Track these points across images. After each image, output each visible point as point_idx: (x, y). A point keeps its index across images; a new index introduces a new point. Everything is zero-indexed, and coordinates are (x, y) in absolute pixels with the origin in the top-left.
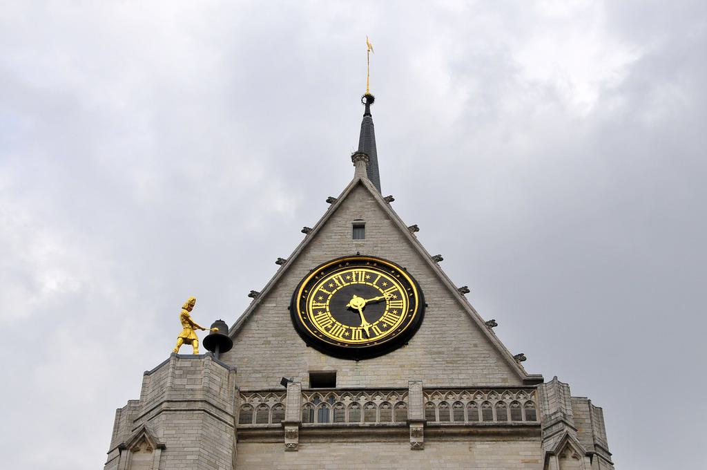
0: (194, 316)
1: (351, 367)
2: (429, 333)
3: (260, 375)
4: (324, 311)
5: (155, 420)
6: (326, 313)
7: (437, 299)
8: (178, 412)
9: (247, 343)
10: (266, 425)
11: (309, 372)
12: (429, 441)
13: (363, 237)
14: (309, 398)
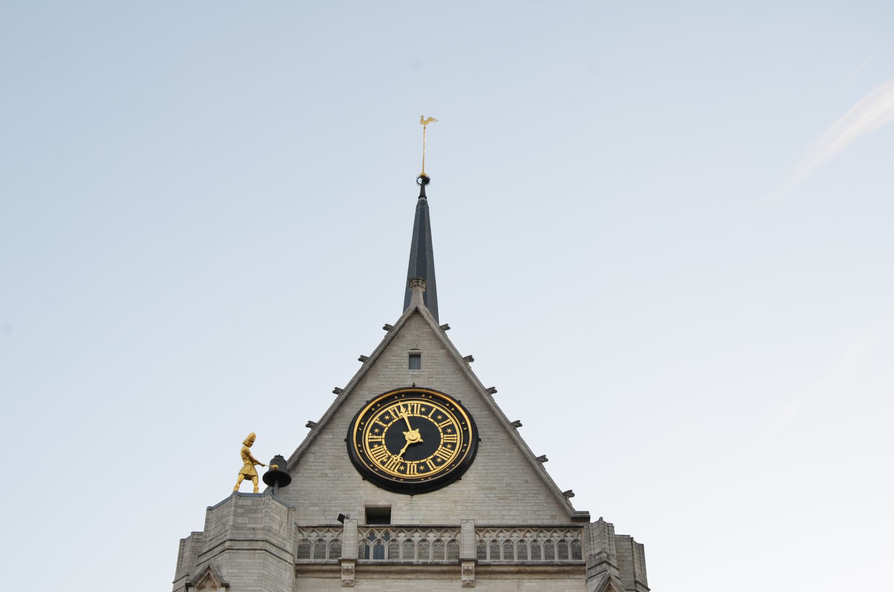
0: (254, 451)
1: (406, 502)
2: (483, 468)
3: (317, 509)
4: (380, 444)
5: (219, 558)
6: (381, 447)
7: (490, 433)
8: (240, 551)
9: (305, 475)
10: (323, 561)
11: (365, 505)
12: (480, 578)
13: (419, 368)
14: (365, 534)
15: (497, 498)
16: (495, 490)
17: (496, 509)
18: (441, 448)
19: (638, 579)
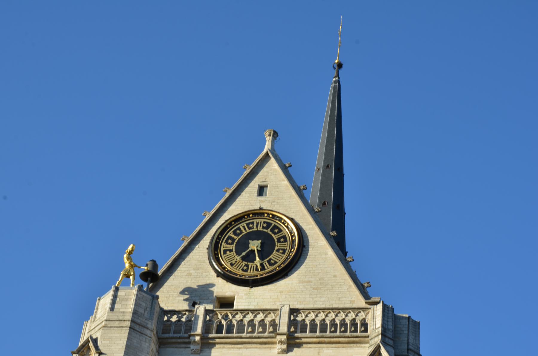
4: (231, 251)
6: (232, 253)
8: (112, 328)
10: (179, 335)
15: (312, 289)
16: (312, 282)
17: (311, 296)
19: (410, 347)
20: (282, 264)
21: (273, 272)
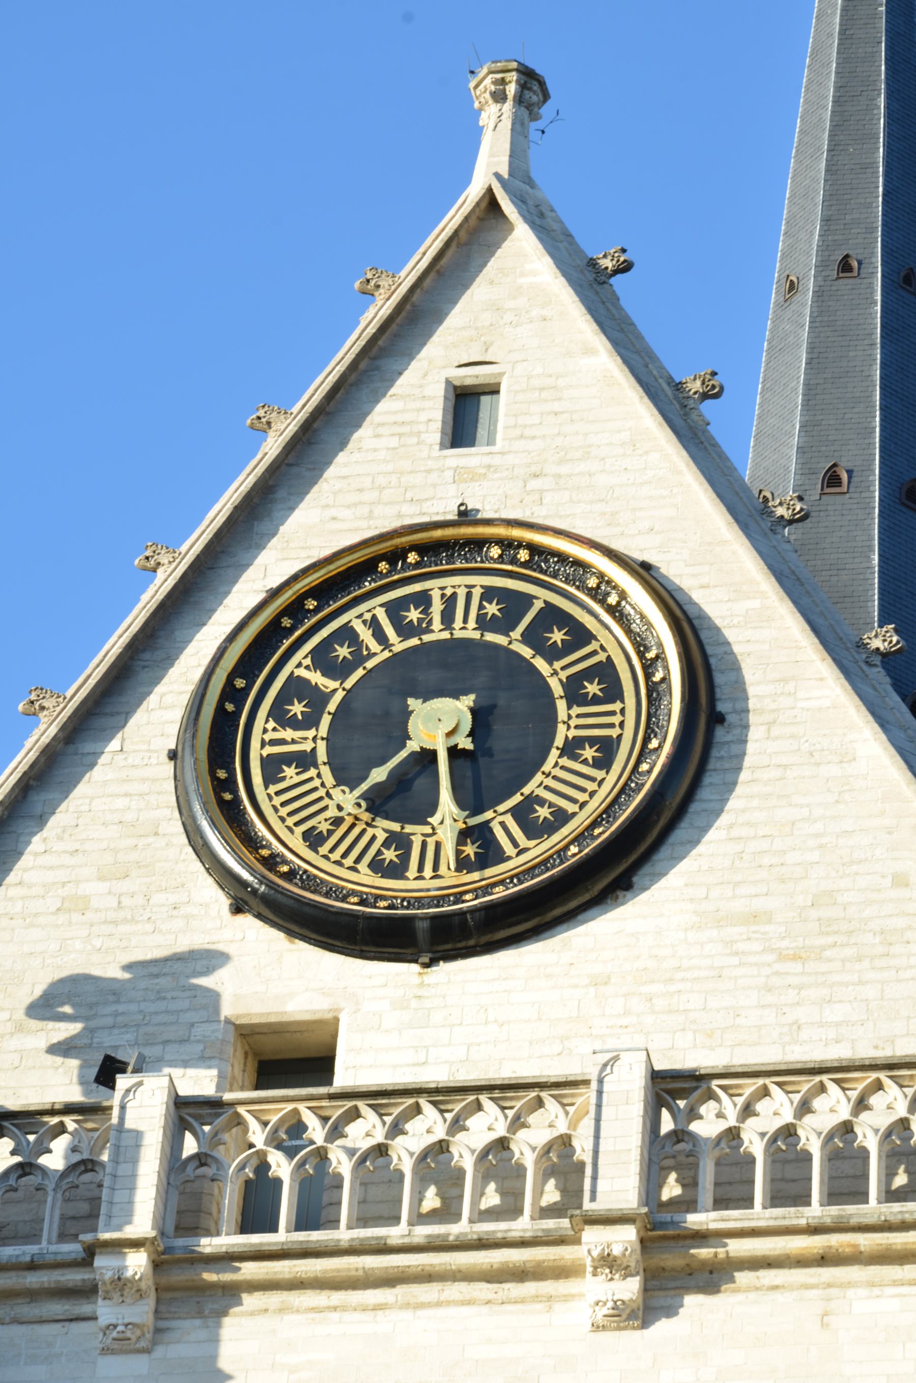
6: (312, 772)
10: (26, 1251)
15: (770, 958)
16: (770, 921)
18: (556, 764)
20: (594, 824)
21: (548, 870)
